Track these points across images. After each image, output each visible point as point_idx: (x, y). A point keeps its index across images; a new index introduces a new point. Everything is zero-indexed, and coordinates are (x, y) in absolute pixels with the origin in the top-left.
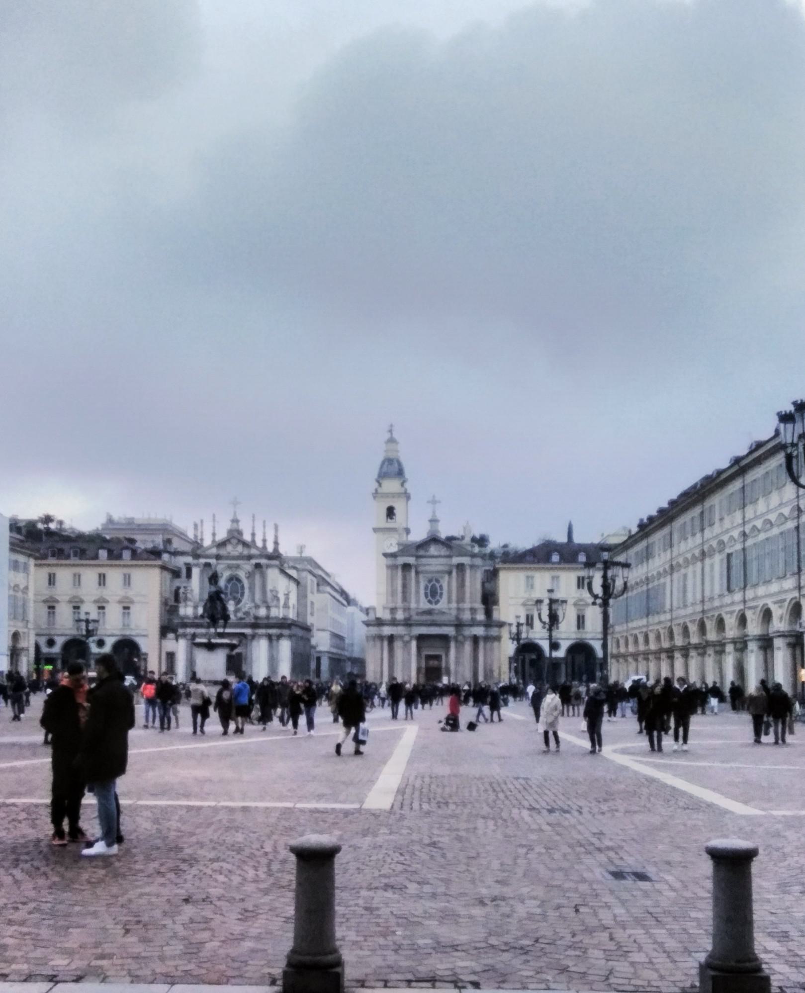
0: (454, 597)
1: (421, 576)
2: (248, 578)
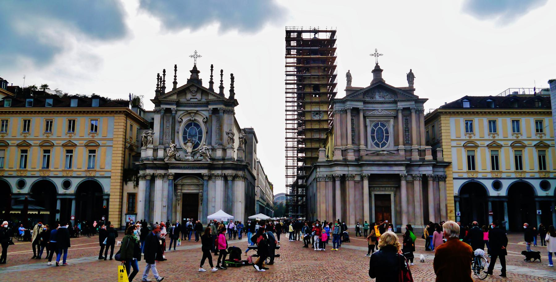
0: (401, 140)
1: (367, 120)
2: (205, 123)
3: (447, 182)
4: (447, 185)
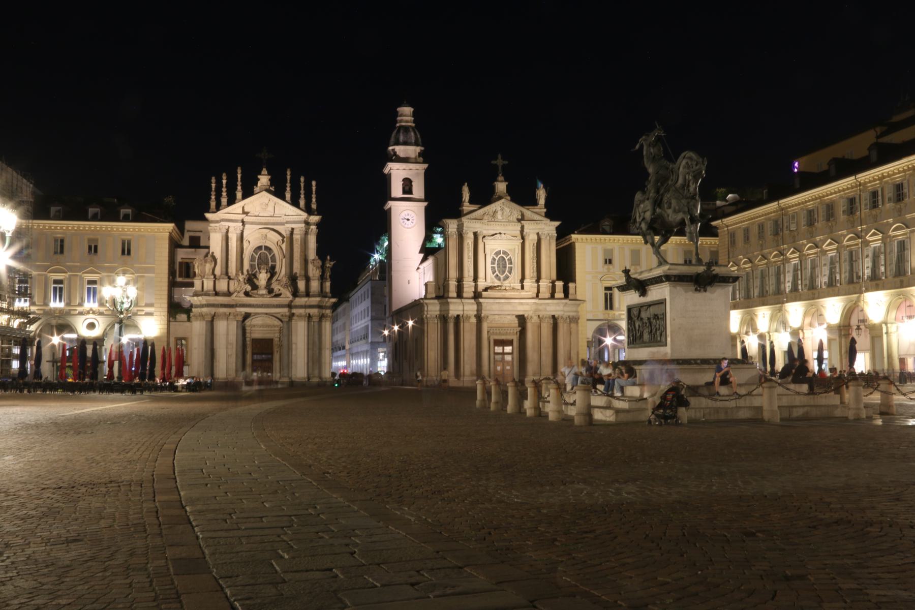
3: (580, 325)
4: (580, 328)
